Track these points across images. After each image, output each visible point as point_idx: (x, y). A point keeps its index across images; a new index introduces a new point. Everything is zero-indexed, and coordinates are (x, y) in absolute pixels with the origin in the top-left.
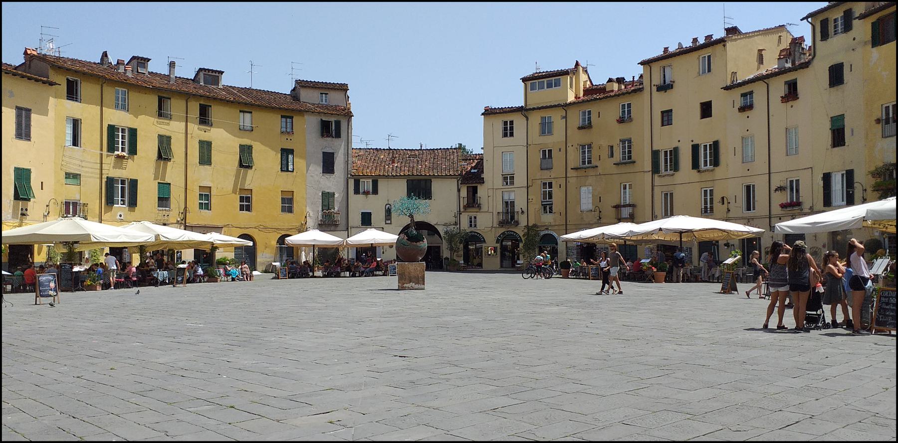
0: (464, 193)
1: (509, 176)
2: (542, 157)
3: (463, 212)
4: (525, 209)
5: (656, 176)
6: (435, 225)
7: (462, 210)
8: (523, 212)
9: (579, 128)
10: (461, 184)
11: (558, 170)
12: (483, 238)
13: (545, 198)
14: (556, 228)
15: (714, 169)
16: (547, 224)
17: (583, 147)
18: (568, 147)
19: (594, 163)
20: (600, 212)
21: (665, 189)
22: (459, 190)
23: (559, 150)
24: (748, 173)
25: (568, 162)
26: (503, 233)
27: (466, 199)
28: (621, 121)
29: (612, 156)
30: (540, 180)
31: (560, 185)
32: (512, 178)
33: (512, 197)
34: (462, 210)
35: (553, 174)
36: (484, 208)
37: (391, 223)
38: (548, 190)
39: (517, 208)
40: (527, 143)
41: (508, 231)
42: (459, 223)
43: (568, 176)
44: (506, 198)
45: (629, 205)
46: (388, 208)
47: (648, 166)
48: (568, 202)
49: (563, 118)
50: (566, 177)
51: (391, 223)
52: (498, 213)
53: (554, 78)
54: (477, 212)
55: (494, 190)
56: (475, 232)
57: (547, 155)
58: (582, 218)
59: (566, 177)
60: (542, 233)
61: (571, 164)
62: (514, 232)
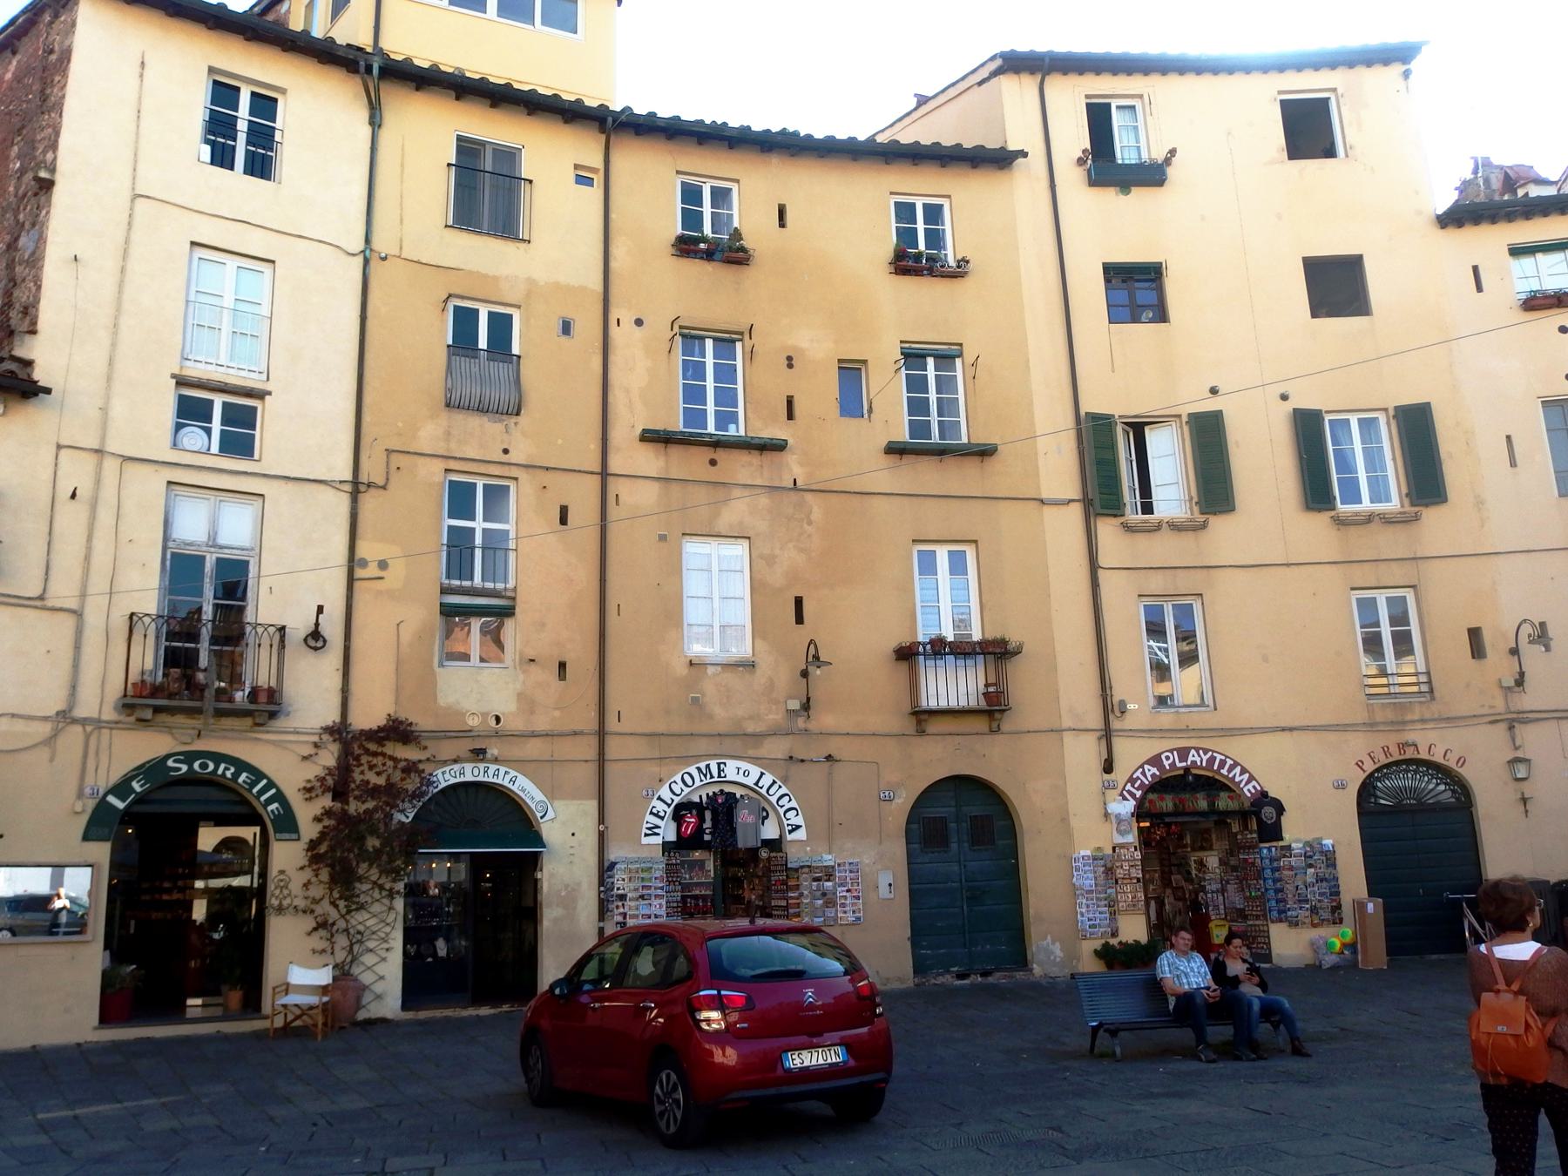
1: (218, 401)
2: (450, 342)
4: (332, 628)
5: (1107, 529)
14: (533, 749)
16: (473, 722)
17: (691, 338)
18: (613, 322)
23: (558, 327)
30: (439, 466)
40: (368, 241)
41: (190, 757)
43: (615, 465)
44: (192, 525)
49: (583, 180)
50: (604, 474)
55: (111, 465)
58: (695, 701)
59: (604, 474)
60: (446, 777)
62: (241, 766)
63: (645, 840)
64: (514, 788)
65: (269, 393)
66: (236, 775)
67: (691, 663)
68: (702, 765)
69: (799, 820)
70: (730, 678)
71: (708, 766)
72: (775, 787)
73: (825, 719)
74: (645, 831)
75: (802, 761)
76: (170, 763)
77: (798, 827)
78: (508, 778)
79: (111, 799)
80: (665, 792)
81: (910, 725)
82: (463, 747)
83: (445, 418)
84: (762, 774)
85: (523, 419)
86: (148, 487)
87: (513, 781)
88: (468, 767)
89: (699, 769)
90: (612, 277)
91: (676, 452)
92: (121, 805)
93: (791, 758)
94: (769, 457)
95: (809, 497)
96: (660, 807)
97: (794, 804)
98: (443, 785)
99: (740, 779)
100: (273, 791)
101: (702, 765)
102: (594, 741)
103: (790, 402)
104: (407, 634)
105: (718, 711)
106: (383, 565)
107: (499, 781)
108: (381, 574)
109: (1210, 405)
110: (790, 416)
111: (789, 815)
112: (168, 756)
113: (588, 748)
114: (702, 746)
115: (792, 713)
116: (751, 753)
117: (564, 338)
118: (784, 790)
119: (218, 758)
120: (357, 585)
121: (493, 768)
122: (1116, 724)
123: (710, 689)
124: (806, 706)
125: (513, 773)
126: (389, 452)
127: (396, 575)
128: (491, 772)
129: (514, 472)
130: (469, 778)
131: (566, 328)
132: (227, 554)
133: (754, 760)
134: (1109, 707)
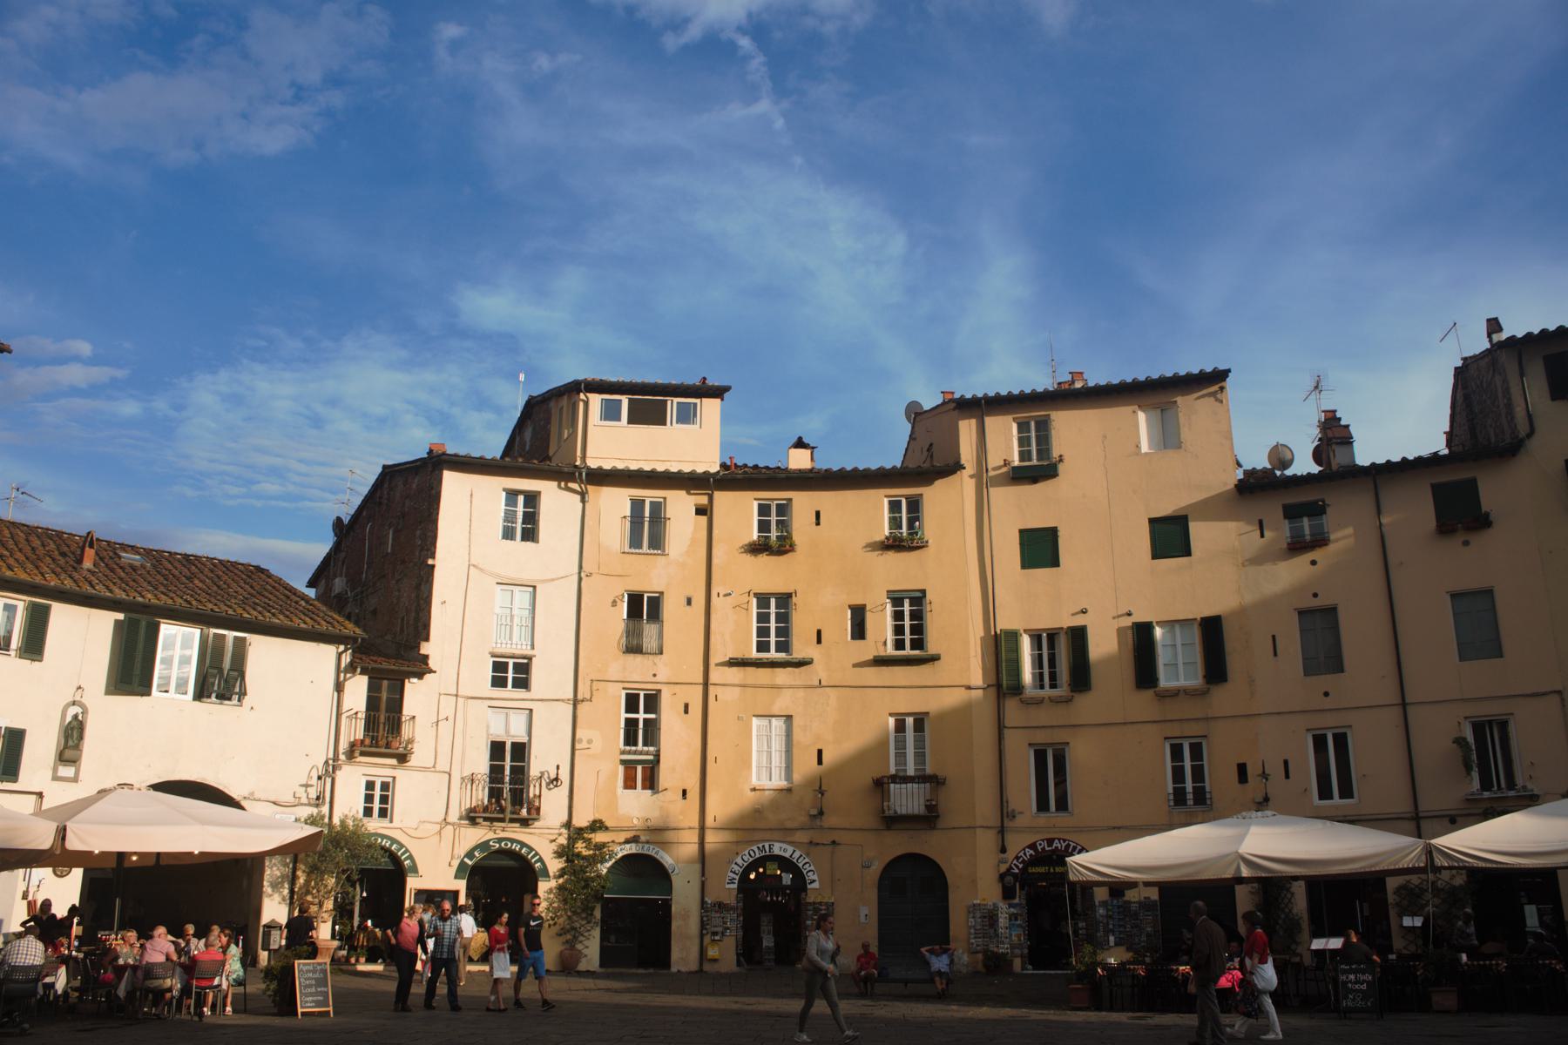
7: (342, 757)
8: (557, 779)
9: (756, 549)
12: (411, 857)
13: (630, 739)
15: (1209, 689)
17: (763, 600)
19: (800, 650)
21: (1041, 737)
22: (339, 687)
24: (1327, 703)
28: (894, 544)
29: (859, 631)
31: (686, 706)
36: (420, 755)
37: (75, 779)
38: (641, 716)
39: (538, 764)
41: (500, 840)
45: (922, 778)
46: (75, 717)
50: (706, 684)
51: (75, 779)
53: (676, 400)
56: (384, 837)
57: (644, 608)
59: (706, 684)
62: (523, 845)
63: (727, 886)
64: (658, 857)
66: (521, 849)
69: (815, 877)
71: (763, 846)
72: (802, 858)
73: (830, 820)
74: (727, 881)
75: (818, 844)
76: (491, 843)
77: (814, 881)
78: (654, 852)
79: (466, 860)
84: (794, 851)
89: (758, 848)
92: (470, 863)
93: (811, 842)
96: (736, 868)
97: (812, 868)
98: (620, 855)
100: (538, 857)
101: (760, 846)
103: (819, 632)
106: (590, 742)
107: (649, 853)
108: (588, 746)
109: (1078, 621)
110: (819, 641)
111: (809, 874)
112: (491, 840)
116: (789, 839)
117: (688, 607)
118: (807, 860)
119: (513, 841)
120: (577, 752)
121: (646, 846)
122: (1007, 823)
124: (821, 813)
125: (657, 849)
127: (597, 746)
128: (645, 848)
130: (634, 851)
131: (689, 602)
133: (790, 843)
134: (1005, 813)
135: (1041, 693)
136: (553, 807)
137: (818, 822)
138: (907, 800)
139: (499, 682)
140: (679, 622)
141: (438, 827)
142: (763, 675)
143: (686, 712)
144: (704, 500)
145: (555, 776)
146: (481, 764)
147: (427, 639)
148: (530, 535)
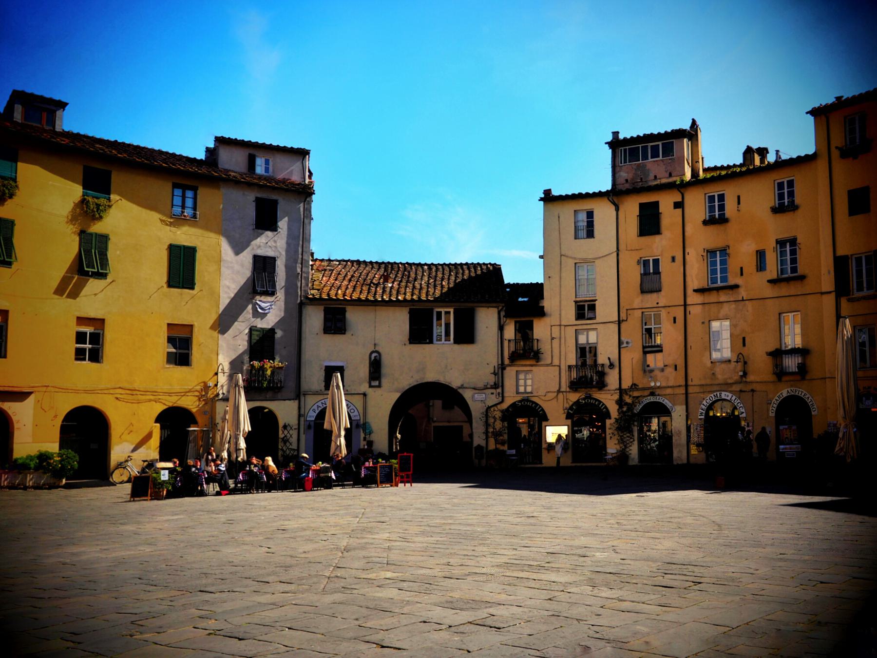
0: (510, 332)
1: (586, 304)
3: (509, 365)
6: (459, 388)
7: (507, 362)
9: (705, 223)
10: (504, 317)
11: (670, 292)
14: (669, 391)
18: (686, 254)
20: (745, 363)
22: (501, 328)
23: (670, 259)
25: (688, 279)
26: (577, 403)
27: (512, 345)
31: (675, 319)
32: (592, 308)
33: (593, 338)
34: (507, 362)
35: (662, 299)
36: (546, 358)
39: (602, 359)
41: (584, 399)
42: (500, 384)
43: (689, 301)
44: (582, 340)
47: (828, 282)
48: (689, 347)
50: (685, 305)
52: (570, 367)
54: (532, 366)
55: (563, 327)
58: (713, 374)
59: (685, 305)
61: (694, 283)
62: (596, 400)
65: (596, 300)
66: (595, 402)
67: (712, 362)
68: (715, 394)
69: (743, 411)
70: (723, 366)
73: (751, 378)
77: (743, 413)
79: (570, 411)
80: (704, 402)
81: (773, 378)
82: (647, 393)
83: (641, 297)
85: (662, 293)
86: (571, 331)
87: (663, 401)
88: (652, 397)
90: (686, 238)
91: (706, 294)
92: (572, 412)
94: (735, 290)
95: (747, 302)
96: (704, 407)
97: (742, 405)
99: (726, 398)
102: (684, 388)
104: (634, 362)
105: (719, 376)
110: (742, 274)
111: (741, 409)
113: (682, 390)
114: (716, 388)
115: (741, 376)
116: (730, 389)
117: (673, 263)
118: (739, 401)
120: (622, 349)
121: (658, 397)
123: (718, 369)
124: (745, 374)
126: (627, 310)
129: (660, 309)
130: (652, 400)
131: (673, 259)
132: (591, 345)
133: (730, 392)
135: (861, 294)
136: (612, 379)
137: (744, 379)
138: (791, 363)
139: (580, 316)
140: (669, 274)
141: (556, 394)
142: (713, 297)
143: (675, 322)
144: (680, 199)
145: (609, 364)
146: (572, 359)
147: (542, 298)
148: (590, 234)
